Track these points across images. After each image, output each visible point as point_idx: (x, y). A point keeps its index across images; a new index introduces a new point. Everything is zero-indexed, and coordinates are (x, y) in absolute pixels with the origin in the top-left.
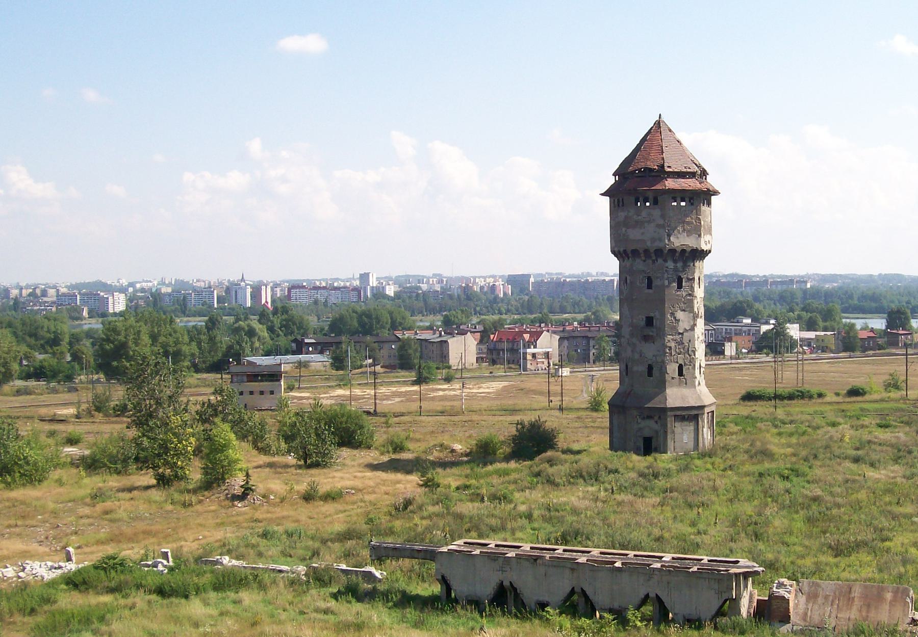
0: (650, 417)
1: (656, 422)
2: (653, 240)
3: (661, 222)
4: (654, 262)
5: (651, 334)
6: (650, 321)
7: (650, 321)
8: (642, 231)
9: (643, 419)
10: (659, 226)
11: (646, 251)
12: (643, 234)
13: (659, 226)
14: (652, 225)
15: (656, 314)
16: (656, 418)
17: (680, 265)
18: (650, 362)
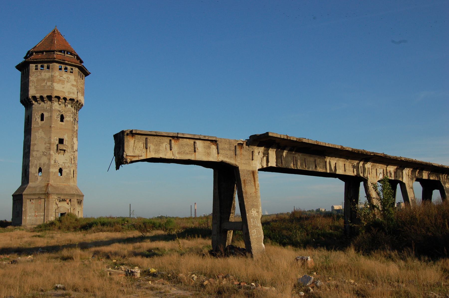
0: (64, 200)
1: (68, 204)
2: (69, 93)
3: (75, 83)
4: (65, 105)
5: (64, 149)
6: (61, 141)
7: (61, 141)
8: (63, 86)
9: (60, 201)
10: (73, 85)
11: (65, 99)
12: (63, 88)
13: (73, 85)
14: (69, 84)
15: (66, 138)
16: (68, 200)
17: (75, 111)
18: (61, 167)
